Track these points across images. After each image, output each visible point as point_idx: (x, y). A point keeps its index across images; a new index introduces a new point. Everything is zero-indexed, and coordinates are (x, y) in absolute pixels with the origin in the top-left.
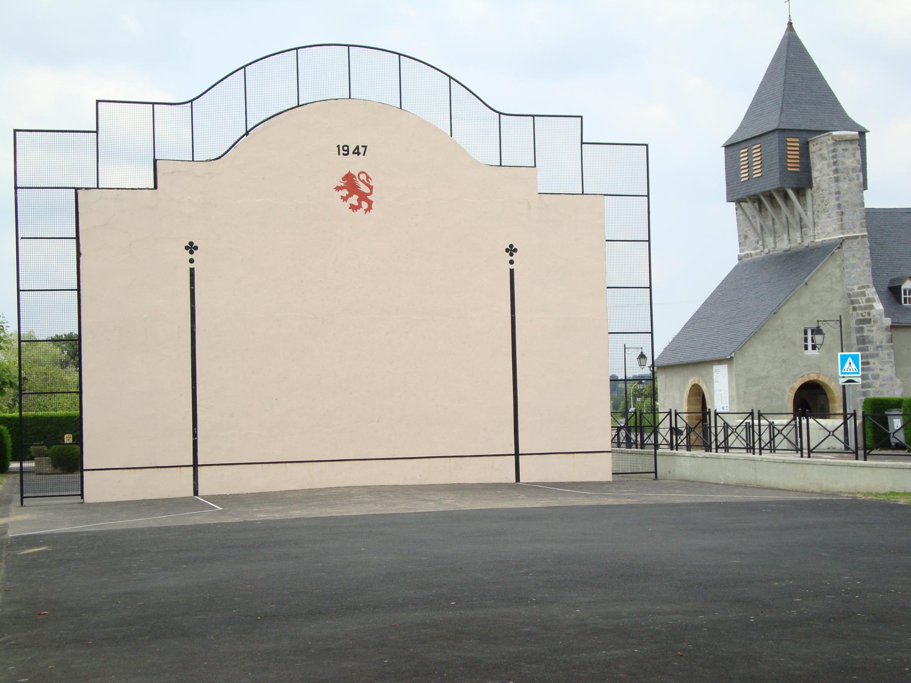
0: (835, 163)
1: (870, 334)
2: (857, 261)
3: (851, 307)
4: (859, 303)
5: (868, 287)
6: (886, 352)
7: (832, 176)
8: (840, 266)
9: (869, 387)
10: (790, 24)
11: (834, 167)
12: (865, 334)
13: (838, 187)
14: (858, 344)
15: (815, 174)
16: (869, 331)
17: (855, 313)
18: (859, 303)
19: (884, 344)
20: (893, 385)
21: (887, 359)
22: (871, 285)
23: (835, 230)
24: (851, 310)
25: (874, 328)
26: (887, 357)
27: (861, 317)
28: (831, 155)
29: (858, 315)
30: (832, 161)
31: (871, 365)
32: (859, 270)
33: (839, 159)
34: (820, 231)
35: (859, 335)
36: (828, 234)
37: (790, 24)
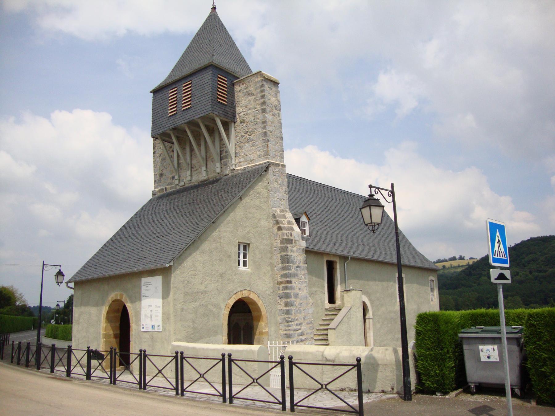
0: (263, 97)
1: (292, 253)
2: (278, 186)
3: (276, 227)
4: (282, 223)
5: (286, 211)
6: (303, 272)
7: (259, 107)
8: (266, 187)
9: (292, 305)
10: (214, 8)
11: (262, 100)
12: (289, 253)
13: (265, 117)
14: (282, 263)
15: (238, 110)
16: (291, 251)
17: (280, 232)
18: (282, 223)
19: (301, 265)
20: (307, 304)
21: (303, 280)
22: (288, 210)
23: (259, 156)
24: (276, 230)
25: (295, 249)
26: (303, 277)
27: (286, 237)
28: (259, 91)
29: (283, 234)
30: (259, 95)
31: (293, 285)
32: (280, 195)
33: (266, 93)
34: (242, 160)
35: (283, 254)
36: (251, 161)
37: (214, 8)
